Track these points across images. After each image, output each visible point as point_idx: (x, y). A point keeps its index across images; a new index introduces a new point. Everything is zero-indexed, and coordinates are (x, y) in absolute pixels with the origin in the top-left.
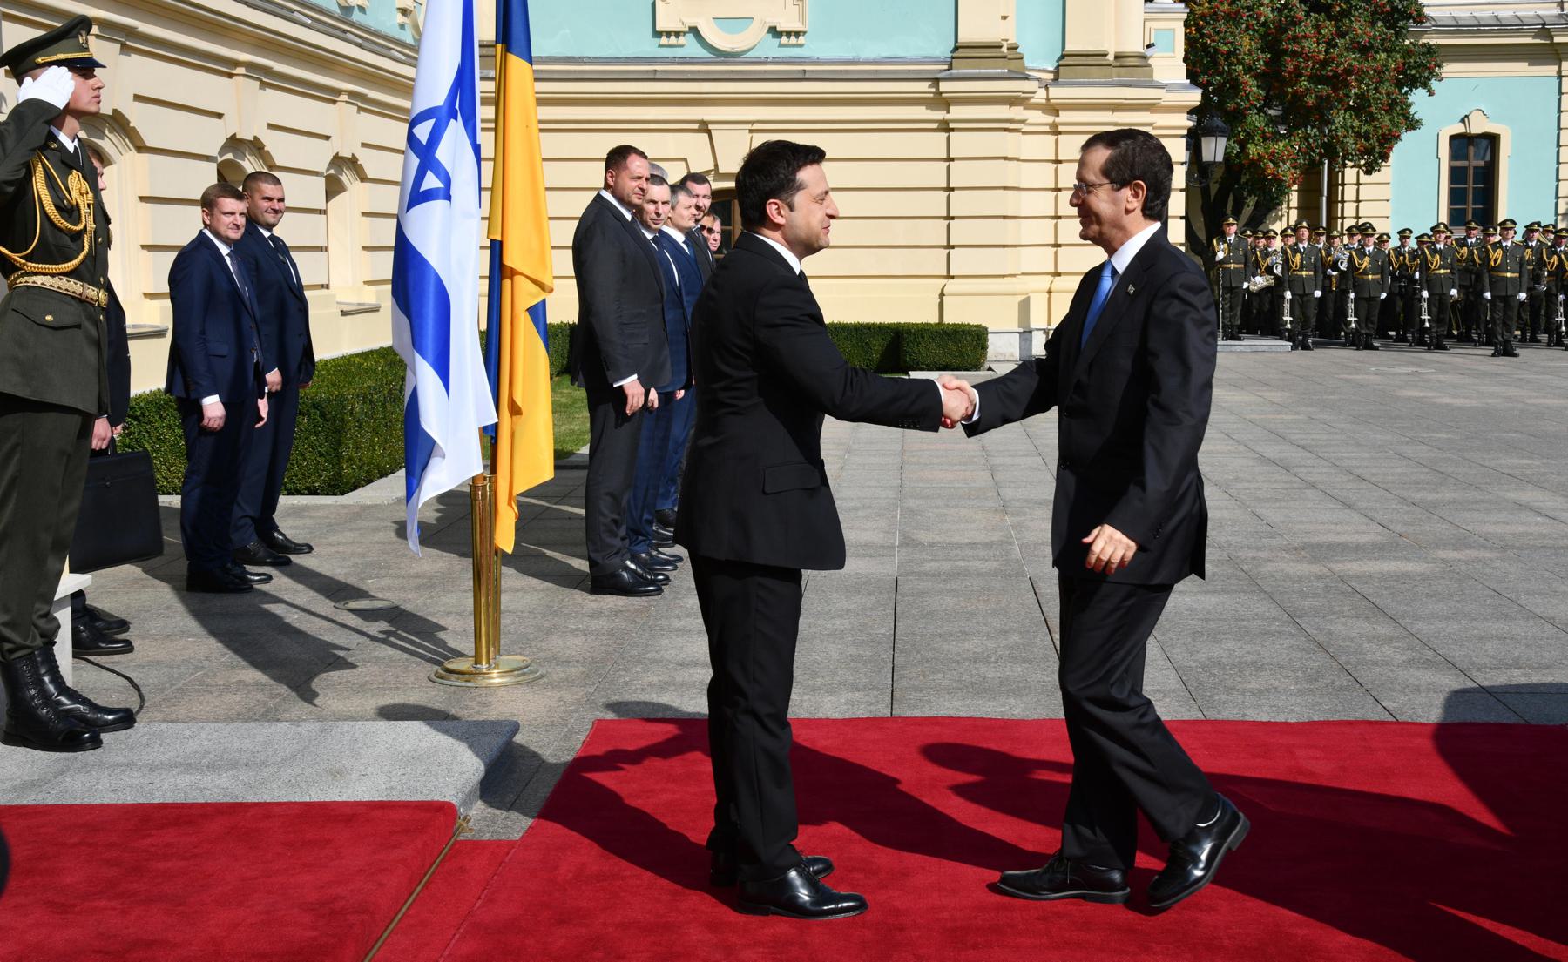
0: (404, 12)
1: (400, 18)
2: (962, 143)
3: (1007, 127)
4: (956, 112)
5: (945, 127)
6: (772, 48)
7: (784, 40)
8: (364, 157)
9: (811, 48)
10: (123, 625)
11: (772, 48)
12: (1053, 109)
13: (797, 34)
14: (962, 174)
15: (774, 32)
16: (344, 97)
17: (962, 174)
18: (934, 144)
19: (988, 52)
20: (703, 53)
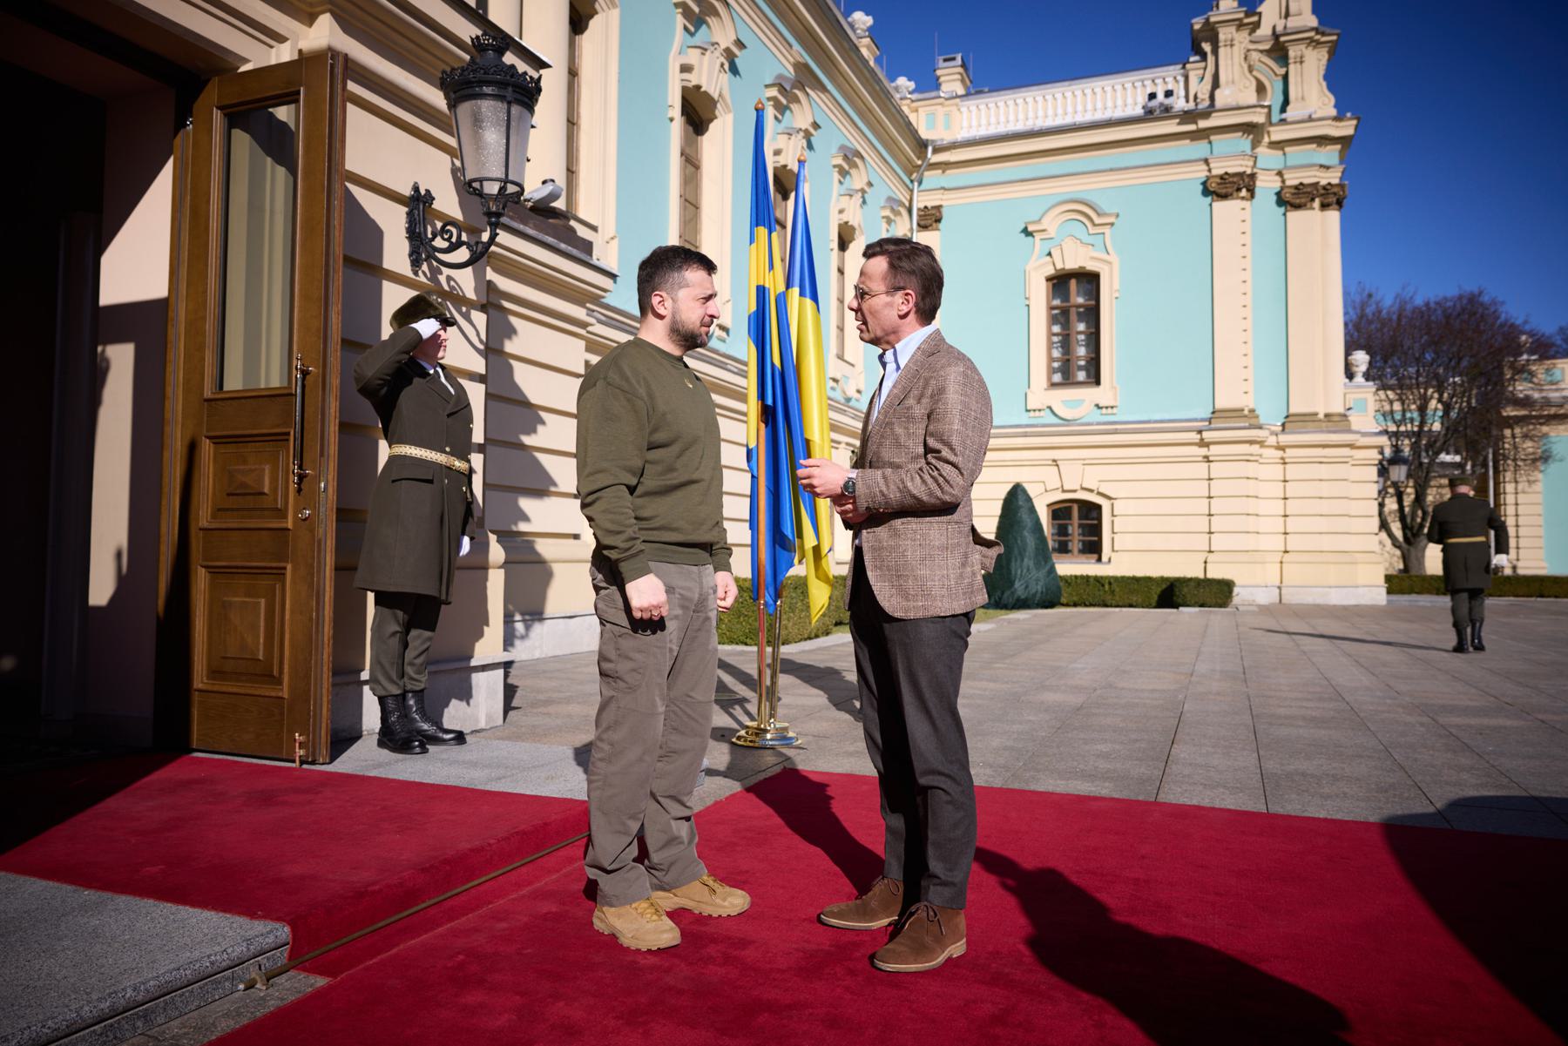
0: (835, 380)
1: (832, 384)
2: (1217, 469)
6: (1097, 416)
11: (1097, 416)
19: (1235, 413)
20: (1055, 420)
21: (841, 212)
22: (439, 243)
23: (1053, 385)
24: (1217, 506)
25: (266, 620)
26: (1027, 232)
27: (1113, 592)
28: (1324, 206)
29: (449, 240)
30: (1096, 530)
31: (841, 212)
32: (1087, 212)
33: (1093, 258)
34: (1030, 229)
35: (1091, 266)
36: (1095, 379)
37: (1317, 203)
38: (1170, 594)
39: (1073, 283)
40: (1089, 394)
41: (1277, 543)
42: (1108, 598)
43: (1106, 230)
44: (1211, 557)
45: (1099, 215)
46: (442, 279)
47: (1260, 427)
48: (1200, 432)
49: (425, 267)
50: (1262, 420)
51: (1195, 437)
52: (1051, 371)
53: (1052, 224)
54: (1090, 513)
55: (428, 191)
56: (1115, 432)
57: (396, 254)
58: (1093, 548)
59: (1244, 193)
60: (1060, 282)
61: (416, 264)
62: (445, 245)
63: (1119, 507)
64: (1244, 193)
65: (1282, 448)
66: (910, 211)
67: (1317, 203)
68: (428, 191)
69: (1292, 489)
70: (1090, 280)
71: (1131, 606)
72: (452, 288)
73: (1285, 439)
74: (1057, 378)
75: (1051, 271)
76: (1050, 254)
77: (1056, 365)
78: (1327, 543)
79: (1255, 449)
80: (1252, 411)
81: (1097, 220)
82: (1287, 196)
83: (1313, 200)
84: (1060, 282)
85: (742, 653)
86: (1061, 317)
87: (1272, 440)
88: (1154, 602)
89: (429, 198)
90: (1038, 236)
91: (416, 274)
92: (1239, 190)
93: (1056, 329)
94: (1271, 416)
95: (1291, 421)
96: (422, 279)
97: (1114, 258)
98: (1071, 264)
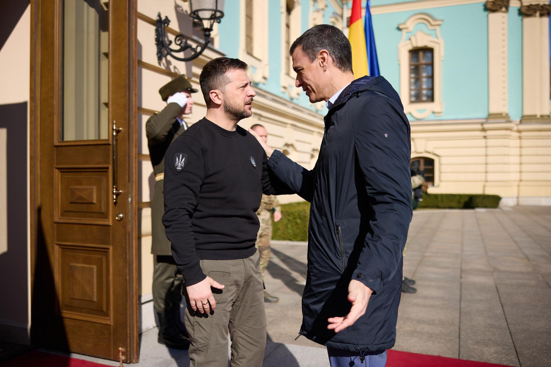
2: (490, 142)
3: (505, 137)
4: (489, 133)
5: (485, 137)
6: (433, 117)
7: (436, 115)
8: (296, 145)
9: (444, 117)
10: (413, 282)
12: (519, 131)
13: (439, 113)
14: (490, 151)
15: (433, 113)
16: (289, 126)
17: (490, 151)
18: (482, 142)
21: (314, 19)
22: (174, 46)
23: (412, 102)
24: (490, 159)
25: (98, 278)
26: (399, 29)
27: (442, 201)
28: (542, 15)
29: (179, 45)
30: (432, 171)
31: (314, 19)
32: (427, 18)
33: (431, 41)
34: (401, 27)
35: (430, 45)
36: (431, 98)
37: (538, 14)
38: (469, 202)
39: (421, 54)
40: (428, 107)
41: (516, 177)
42: (440, 204)
43: (438, 28)
44: (488, 184)
45: (435, 20)
46: (172, 68)
47: (510, 122)
48: (482, 124)
49: (164, 61)
50: (512, 118)
51: (479, 127)
52: (411, 96)
53: (411, 24)
54: (430, 162)
55: (166, 17)
56: (442, 124)
57: (149, 53)
58: (430, 179)
59: (504, 9)
60: (415, 52)
61: (160, 59)
62: (178, 48)
63: (444, 160)
64: (504, 9)
65: (519, 131)
66: (342, 17)
67: (538, 14)
68: (166, 17)
69: (524, 151)
70: (429, 51)
71: (450, 208)
72: (176, 70)
73: (522, 127)
74: (413, 99)
75: (410, 47)
76: (410, 39)
77: (413, 93)
78: (541, 176)
79: (508, 132)
80: (507, 114)
81: (433, 23)
82: (524, 10)
83: (536, 12)
84: (415, 52)
85: (293, 247)
86: (416, 70)
87: (515, 128)
88: (462, 205)
89: (167, 21)
90: (404, 31)
91: (160, 64)
92: (501, 8)
93: (413, 76)
94: (515, 117)
95: (525, 119)
96: (163, 67)
97: (441, 41)
98: (421, 43)
